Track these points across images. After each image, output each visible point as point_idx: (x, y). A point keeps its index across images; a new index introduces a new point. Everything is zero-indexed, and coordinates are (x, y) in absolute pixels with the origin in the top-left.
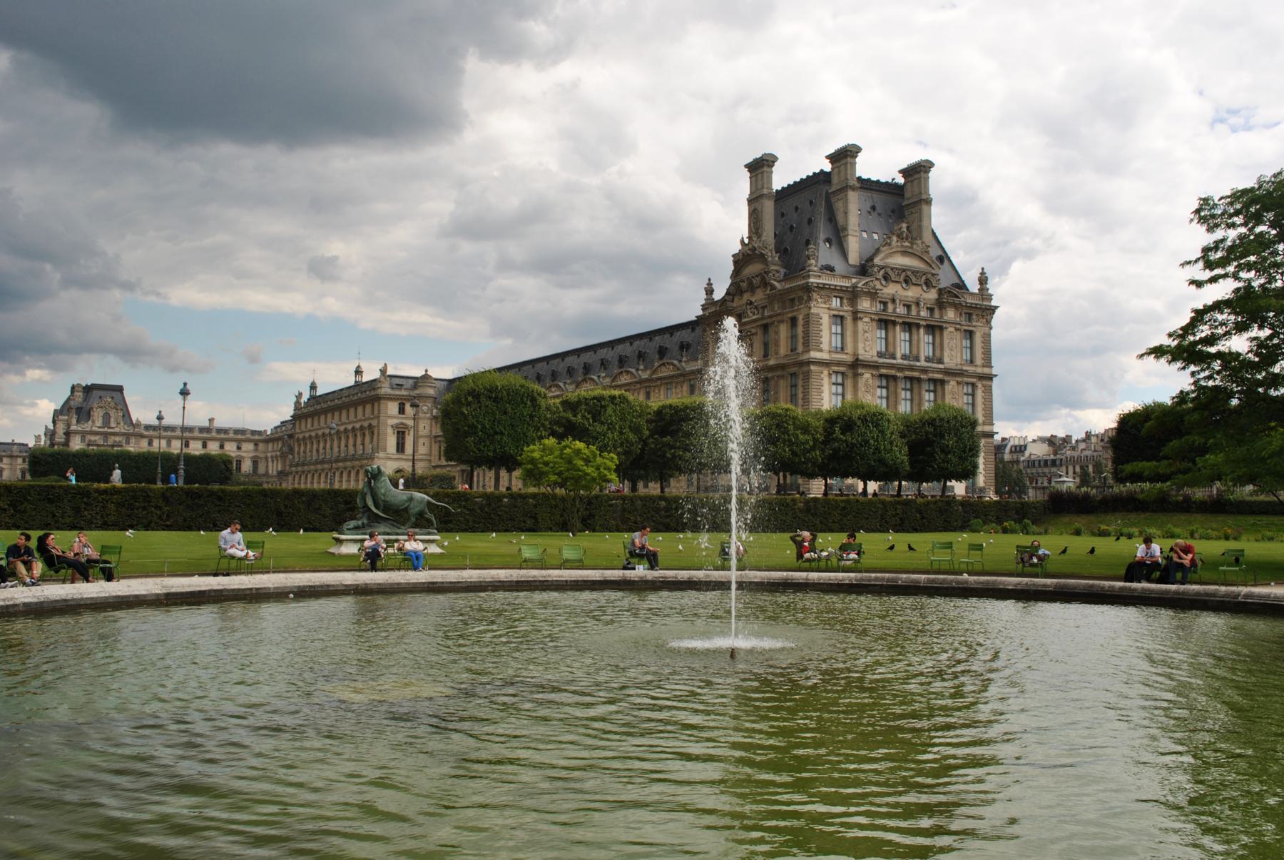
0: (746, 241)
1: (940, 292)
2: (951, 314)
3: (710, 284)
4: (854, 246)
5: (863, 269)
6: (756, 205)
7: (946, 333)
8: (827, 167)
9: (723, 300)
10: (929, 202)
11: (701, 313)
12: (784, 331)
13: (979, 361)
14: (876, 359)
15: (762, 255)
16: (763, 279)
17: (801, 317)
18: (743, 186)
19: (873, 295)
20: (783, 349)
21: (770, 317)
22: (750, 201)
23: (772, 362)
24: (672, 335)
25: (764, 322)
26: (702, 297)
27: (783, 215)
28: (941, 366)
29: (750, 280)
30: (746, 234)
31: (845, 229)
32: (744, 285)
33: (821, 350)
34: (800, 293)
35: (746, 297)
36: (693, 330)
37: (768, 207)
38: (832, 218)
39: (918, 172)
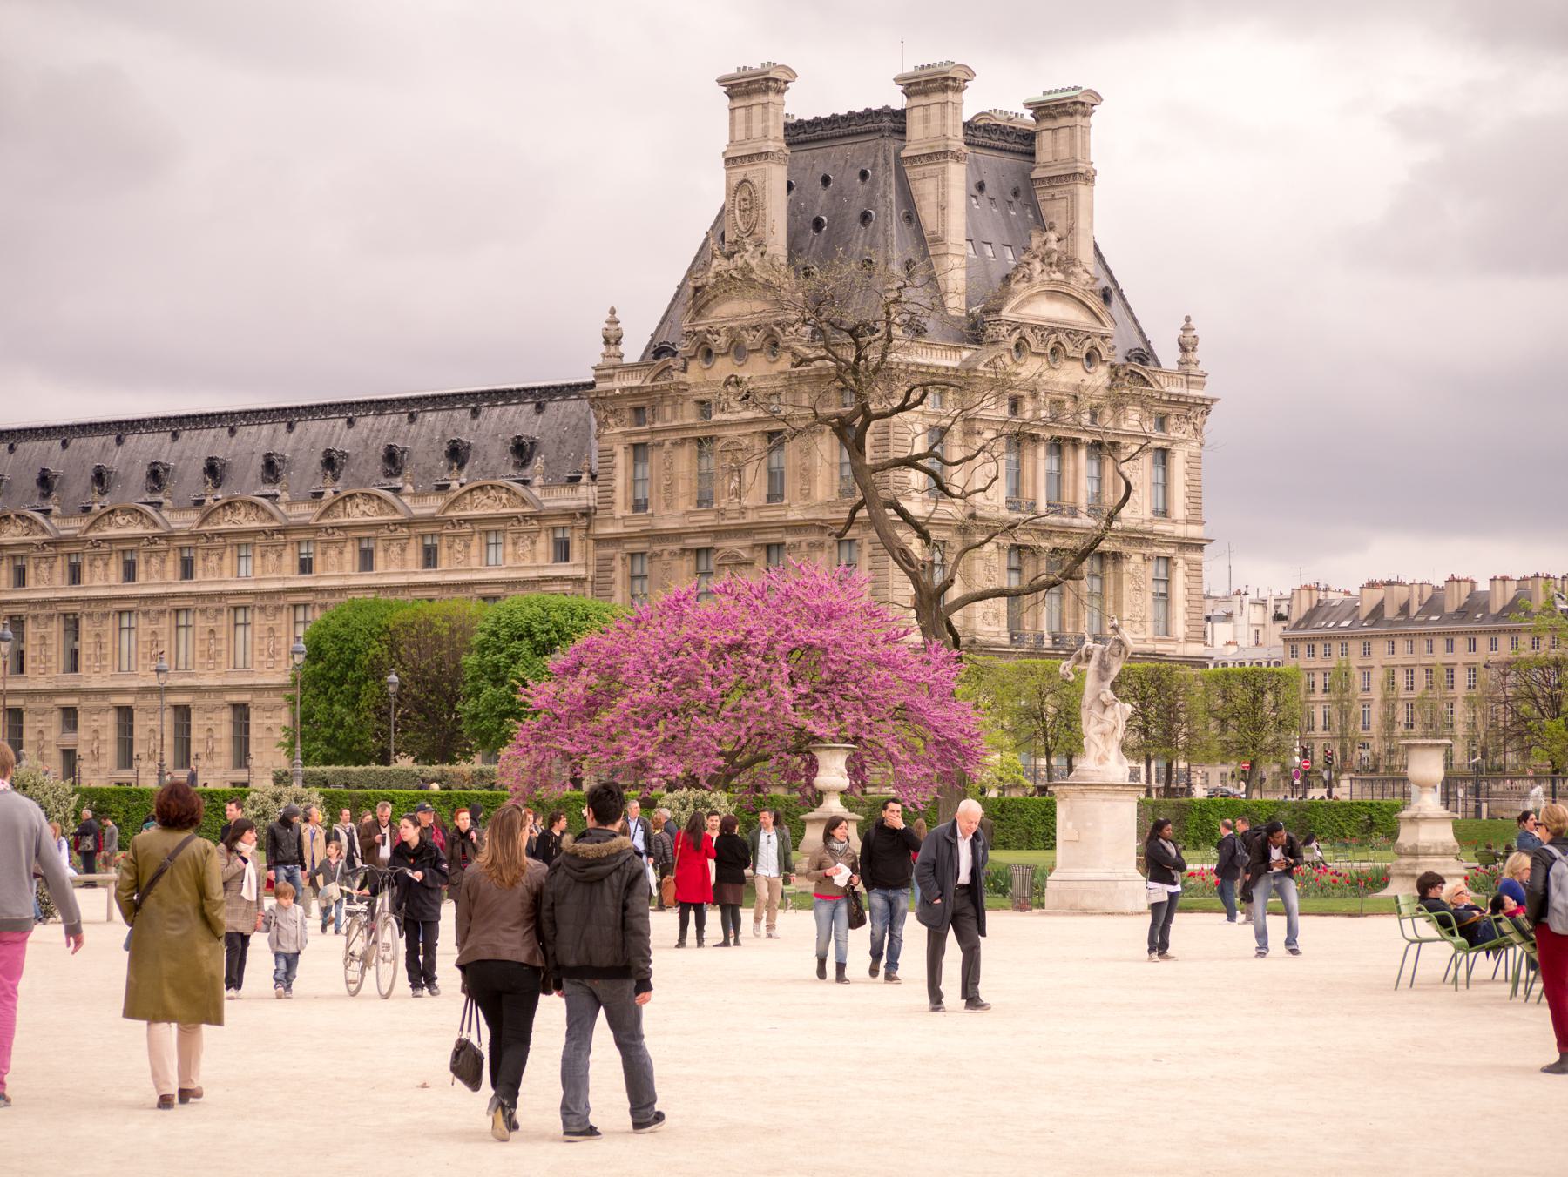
2: (1133, 420)
4: (956, 277)
5: (974, 332)
6: (739, 173)
8: (898, 101)
10: (1089, 178)
13: (1179, 510)
14: (1004, 513)
18: (714, 123)
22: (730, 161)
23: (795, 514)
24: (475, 413)
26: (596, 352)
31: (938, 241)
35: (723, 367)
36: (540, 408)
37: (774, 179)
38: (911, 216)
39: (1065, 110)
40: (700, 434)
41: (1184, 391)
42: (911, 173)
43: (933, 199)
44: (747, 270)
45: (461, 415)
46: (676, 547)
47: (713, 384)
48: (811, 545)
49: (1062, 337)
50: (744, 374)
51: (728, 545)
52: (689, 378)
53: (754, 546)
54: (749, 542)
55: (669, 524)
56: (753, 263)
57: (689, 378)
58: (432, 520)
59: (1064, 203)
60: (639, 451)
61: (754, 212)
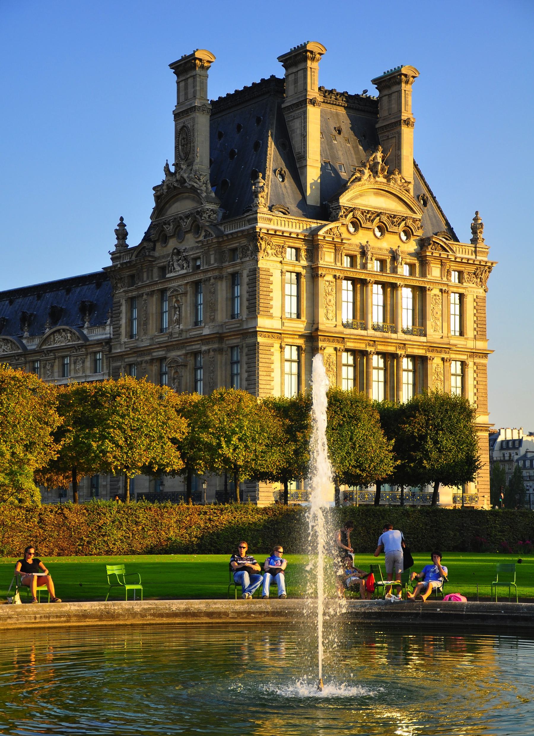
0: (172, 169)
1: (423, 243)
3: (122, 225)
7: (430, 295)
8: (280, 73)
9: (140, 249)
11: (110, 263)
12: (222, 289)
14: (340, 328)
15: (194, 190)
16: (195, 220)
17: (245, 273)
19: (337, 248)
20: (221, 316)
21: (205, 271)
22: (177, 116)
23: (206, 331)
25: (196, 278)
27: (220, 135)
28: (423, 339)
29: (177, 221)
30: (172, 161)
32: (169, 229)
33: (271, 316)
34: (244, 242)
36: (98, 285)
37: (202, 124)
40: (160, 287)
41: (473, 257)
42: (287, 117)
43: (298, 132)
44: (182, 181)
45: (62, 292)
46: (148, 358)
47: (168, 255)
48: (214, 350)
49: (384, 218)
50: (182, 247)
51: (173, 354)
52: (156, 254)
53: (186, 355)
54: (184, 352)
55: (146, 343)
56: (185, 176)
57: (156, 254)
58: (34, 352)
59: (394, 140)
60: (132, 301)
61: (189, 145)
